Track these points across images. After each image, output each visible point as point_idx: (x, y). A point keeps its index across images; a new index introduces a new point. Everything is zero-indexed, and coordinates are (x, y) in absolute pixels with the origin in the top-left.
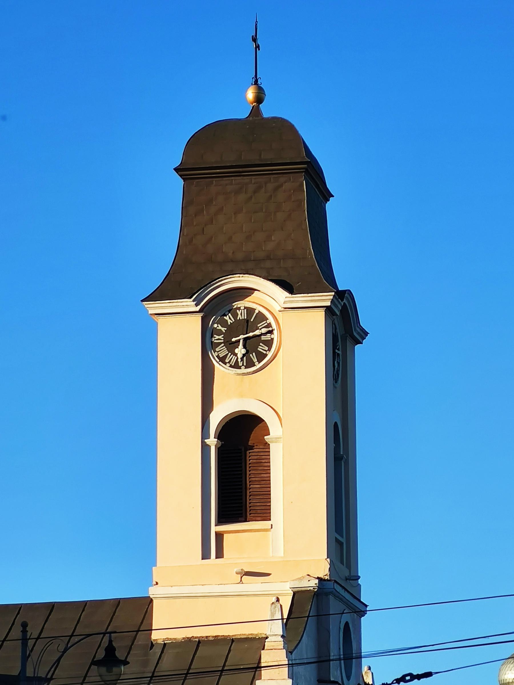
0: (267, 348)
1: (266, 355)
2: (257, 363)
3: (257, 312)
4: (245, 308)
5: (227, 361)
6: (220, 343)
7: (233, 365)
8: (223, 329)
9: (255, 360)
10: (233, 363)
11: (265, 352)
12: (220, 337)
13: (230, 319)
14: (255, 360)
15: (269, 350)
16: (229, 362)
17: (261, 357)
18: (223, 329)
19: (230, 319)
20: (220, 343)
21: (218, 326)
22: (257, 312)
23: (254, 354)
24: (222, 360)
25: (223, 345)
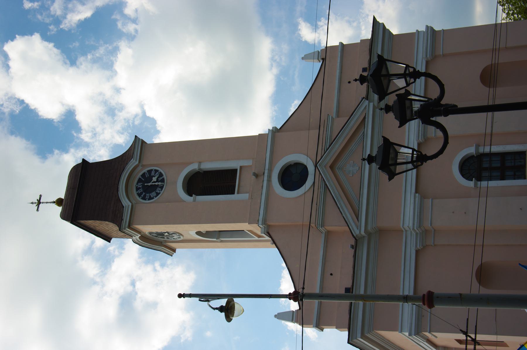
1: (160, 172)
2: (163, 177)
3: (140, 177)
4: (137, 184)
5: (159, 192)
6: (150, 195)
7: (161, 189)
8: (144, 194)
9: (161, 178)
12: (147, 195)
13: (140, 190)
14: (161, 178)
16: (160, 191)
18: (144, 194)
20: (150, 195)
24: (158, 194)
25: (151, 194)
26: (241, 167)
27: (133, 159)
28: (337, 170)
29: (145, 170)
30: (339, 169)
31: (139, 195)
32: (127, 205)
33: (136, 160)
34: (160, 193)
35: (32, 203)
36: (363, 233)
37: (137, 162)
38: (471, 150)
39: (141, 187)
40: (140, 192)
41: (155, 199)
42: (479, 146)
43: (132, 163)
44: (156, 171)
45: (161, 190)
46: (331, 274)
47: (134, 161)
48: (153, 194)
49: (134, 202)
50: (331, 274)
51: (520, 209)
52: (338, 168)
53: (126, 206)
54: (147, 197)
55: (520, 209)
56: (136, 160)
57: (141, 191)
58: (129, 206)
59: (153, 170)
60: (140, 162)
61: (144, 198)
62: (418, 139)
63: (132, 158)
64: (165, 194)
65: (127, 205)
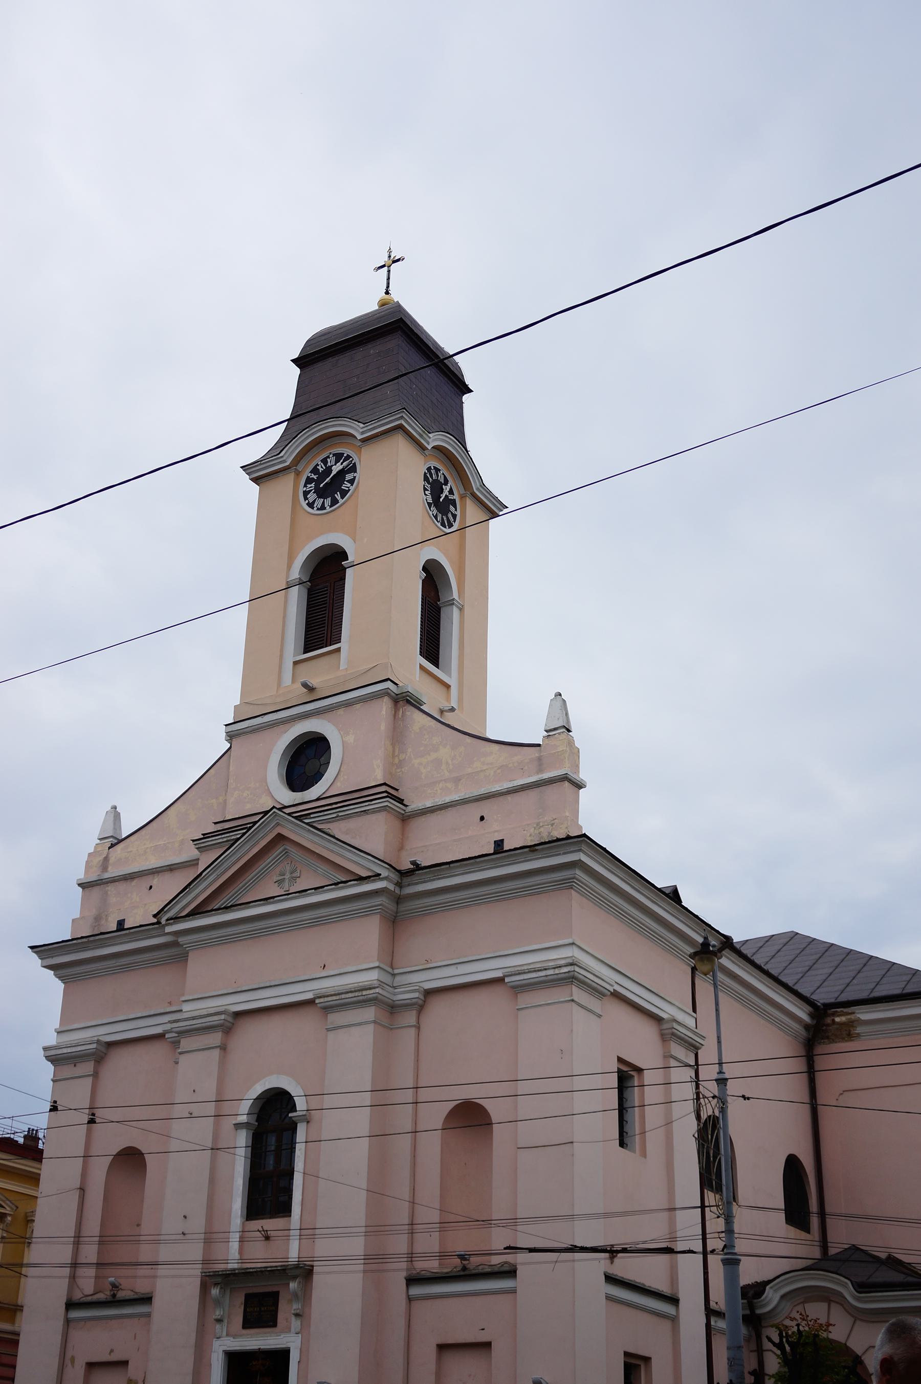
0: (349, 485)
1: (349, 490)
3: (345, 455)
4: (334, 455)
5: (315, 506)
8: (315, 477)
10: (319, 506)
11: (347, 489)
13: (322, 467)
15: (352, 485)
16: (317, 507)
17: (344, 493)
18: (315, 477)
19: (322, 467)
21: (311, 475)
22: (345, 455)
23: (338, 493)
25: (313, 491)
26: (339, 650)
27: (362, 425)
28: (281, 849)
29: (356, 459)
30: (287, 852)
31: (315, 470)
32: (284, 458)
33: (363, 433)
34: (313, 508)
35: (390, 251)
36: (168, 929)
37: (359, 437)
38: (301, 1104)
39: (329, 464)
40: (319, 467)
41: (304, 504)
42: (308, 1122)
43: (357, 430)
44: (352, 482)
45: (318, 509)
46: (151, 887)
47: (361, 430)
48: (312, 496)
49: (300, 468)
50: (151, 887)
51: (185, 1217)
52: (285, 849)
53: (282, 457)
54: (309, 486)
55: (185, 1217)
56: (363, 433)
57: (321, 470)
58: (284, 461)
59: (355, 474)
60: (364, 440)
61: (309, 481)
62: (320, 997)
63: (364, 424)
64: (309, 517)
65: (284, 458)
